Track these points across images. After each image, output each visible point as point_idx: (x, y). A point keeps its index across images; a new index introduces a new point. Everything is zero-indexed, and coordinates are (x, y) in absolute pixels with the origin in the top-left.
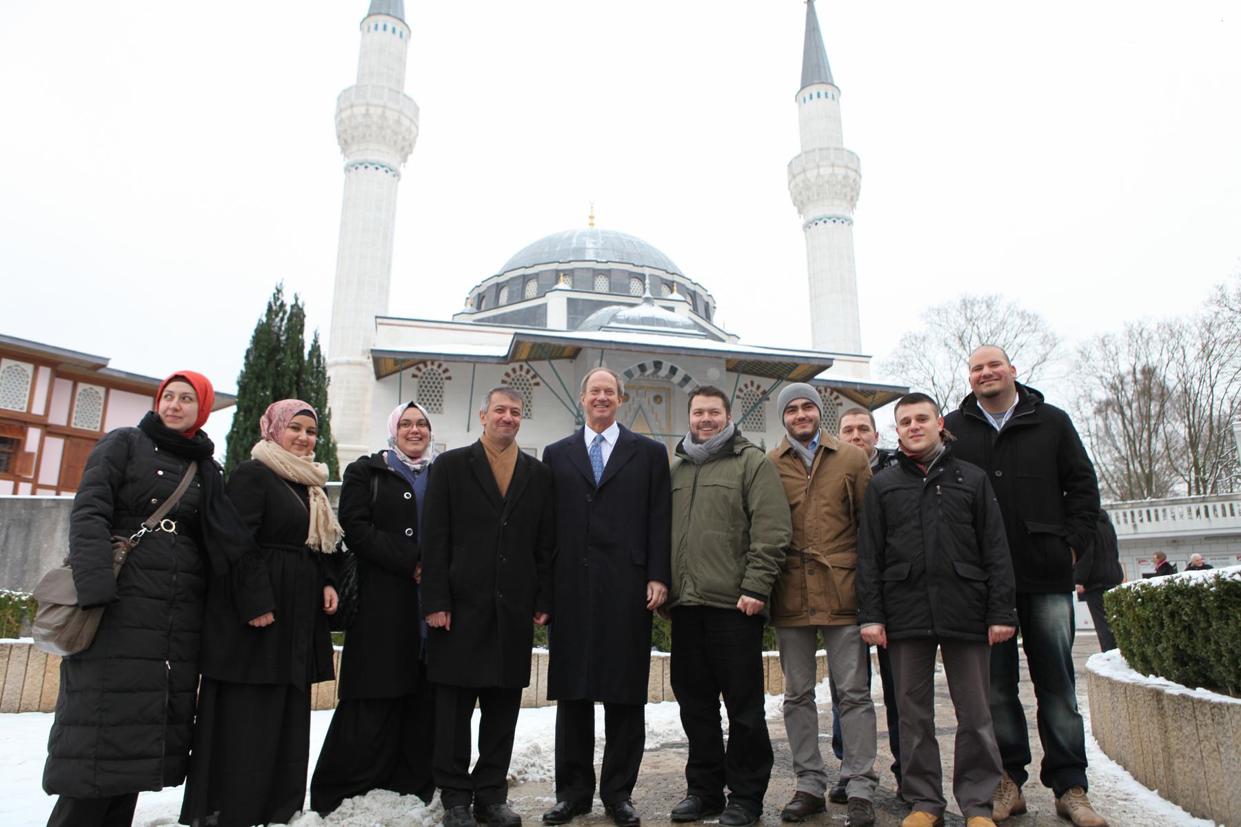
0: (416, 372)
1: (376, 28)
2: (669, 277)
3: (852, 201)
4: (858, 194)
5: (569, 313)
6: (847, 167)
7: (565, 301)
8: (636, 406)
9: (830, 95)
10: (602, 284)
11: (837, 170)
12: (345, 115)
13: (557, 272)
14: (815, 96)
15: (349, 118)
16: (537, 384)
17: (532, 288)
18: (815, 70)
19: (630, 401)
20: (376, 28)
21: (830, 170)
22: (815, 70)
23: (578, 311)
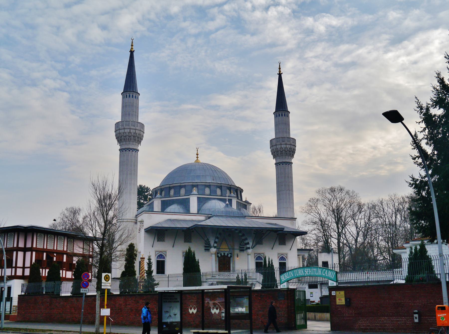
1: (129, 97)
2: (229, 186)
3: (292, 156)
4: (295, 153)
5: (198, 202)
6: (291, 145)
7: (196, 198)
9: (286, 115)
10: (207, 191)
11: (287, 146)
13: (192, 185)
16: (193, 231)
17: (183, 191)
20: (129, 97)
21: (285, 146)
23: (201, 202)
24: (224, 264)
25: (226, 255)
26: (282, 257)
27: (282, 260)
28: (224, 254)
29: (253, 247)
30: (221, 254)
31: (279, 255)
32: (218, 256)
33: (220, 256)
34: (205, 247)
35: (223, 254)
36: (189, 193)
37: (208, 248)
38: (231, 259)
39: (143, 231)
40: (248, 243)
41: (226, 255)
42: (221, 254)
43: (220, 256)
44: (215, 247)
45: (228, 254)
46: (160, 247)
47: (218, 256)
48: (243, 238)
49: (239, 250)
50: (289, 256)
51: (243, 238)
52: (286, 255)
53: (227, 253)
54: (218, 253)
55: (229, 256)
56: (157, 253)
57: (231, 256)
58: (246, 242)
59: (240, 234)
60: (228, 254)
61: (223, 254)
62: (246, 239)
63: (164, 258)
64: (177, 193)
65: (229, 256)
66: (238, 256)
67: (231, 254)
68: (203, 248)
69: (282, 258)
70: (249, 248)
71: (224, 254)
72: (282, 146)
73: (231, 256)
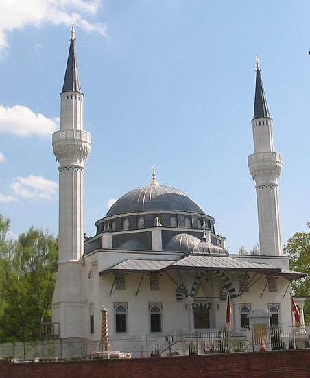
1: (67, 98)
10: (173, 221)
12: (57, 145)
14: (262, 124)
15: (59, 146)
18: (260, 110)
20: (67, 98)
22: (260, 110)
24: (202, 318)
25: (203, 305)
27: (273, 311)
28: (201, 304)
29: (239, 296)
30: (197, 305)
33: (195, 307)
34: (177, 295)
35: (199, 305)
36: (150, 224)
38: (210, 311)
39: (96, 277)
40: (234, 290)
41: (203, 305)
42: (197, 305)
44: (192, 296)
45: (206, 305)
46: (120, 296)
48: (227, 283)
49: (219, 300)
51: (227, 283)
53: (206, 302)
55: (208, 307)
56: (116, 304)
58: (231, 288)
59: (224, 278)
60: (206, 305)
61: (199, 305)
62: (231, 284)
63: (125, 311)
64: (134, 225)
65: (208, 307)
66: (218, 307)
67: (210, 304)
68: (174, 298)
69: (273, 309)
70: (235, 296)
71: (201, 304)
72: (266, 163)
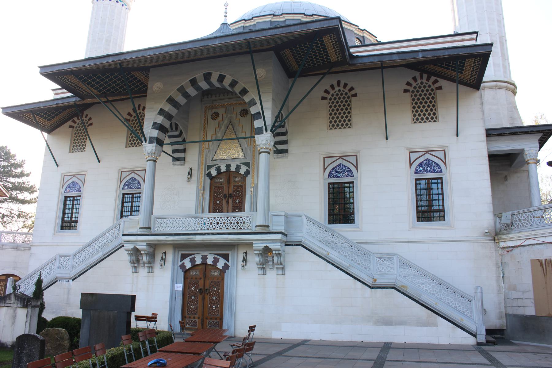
0: (72, 124)
8: (226, 122)
19: (220, 118)
25: (233, 169)
26: (428, 161)
27: (425, 171)
28: (228, 166)
30: (218, 169)
31: (414, 156)
32: (209, 175)
33: (214, 172)
35: (223, 169)
37: (181, 155)
38: (249, 178)
41: (233, 169)
42: (218, 169)
43: (214, 172)
45: (238, 167)
47: (209, 175)
50: (452, 156)
52: (441, 154)
54: (209, 167)
55: (242, 171)
57: (247, 172)
60: (238, 167)
61: (223, 169)
65: (242, 171)
67: (248, 165)
71: (228, 166)
73: (247, 172)
